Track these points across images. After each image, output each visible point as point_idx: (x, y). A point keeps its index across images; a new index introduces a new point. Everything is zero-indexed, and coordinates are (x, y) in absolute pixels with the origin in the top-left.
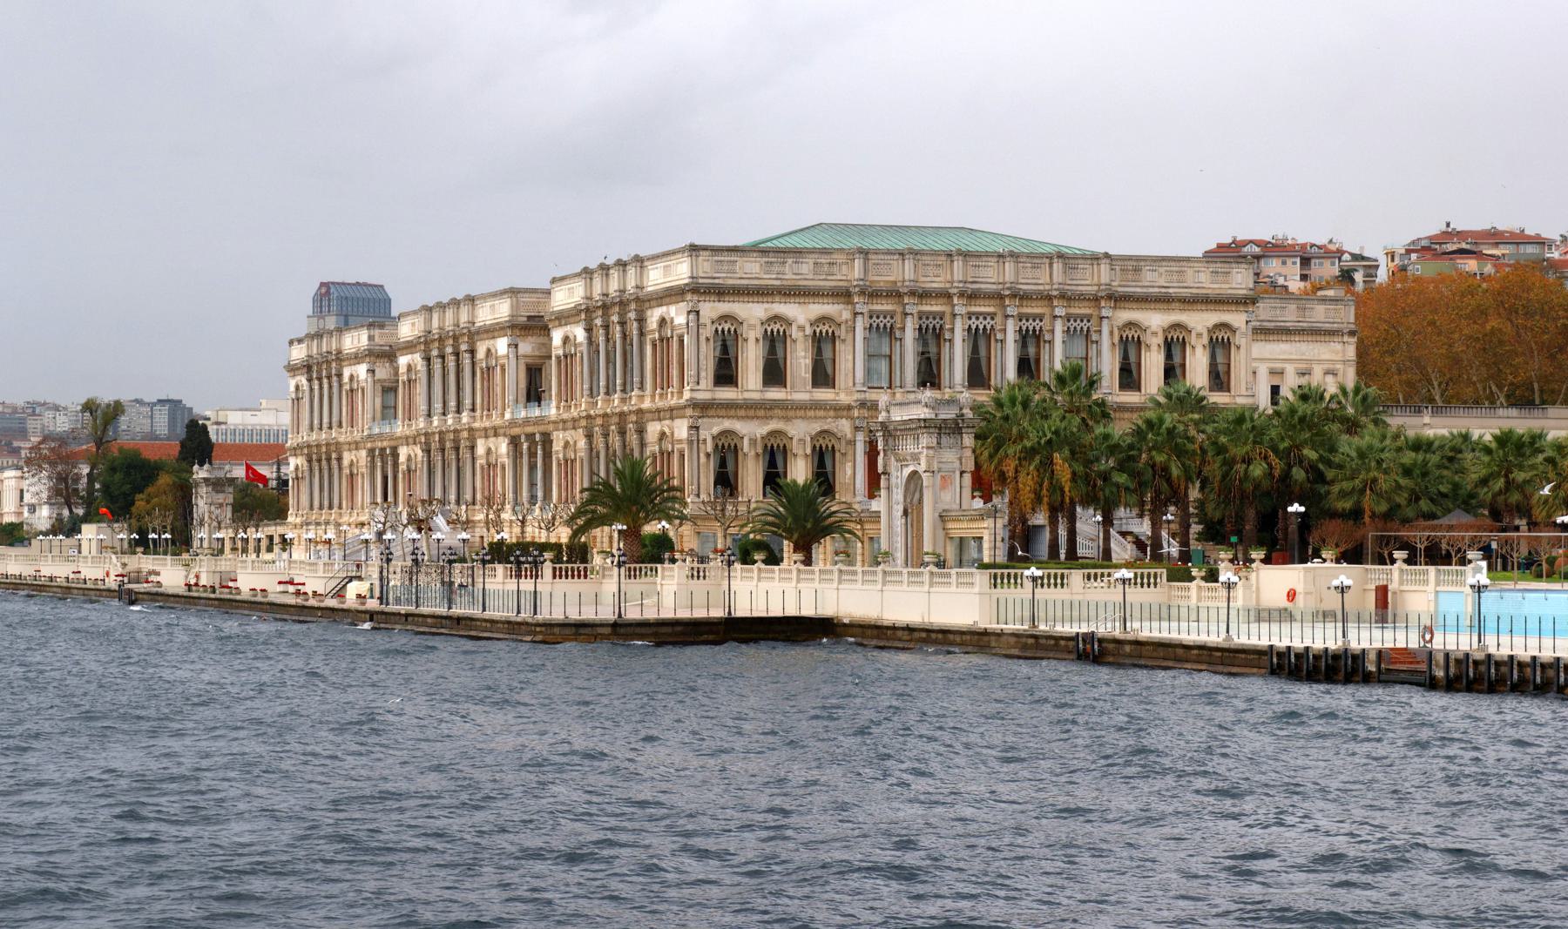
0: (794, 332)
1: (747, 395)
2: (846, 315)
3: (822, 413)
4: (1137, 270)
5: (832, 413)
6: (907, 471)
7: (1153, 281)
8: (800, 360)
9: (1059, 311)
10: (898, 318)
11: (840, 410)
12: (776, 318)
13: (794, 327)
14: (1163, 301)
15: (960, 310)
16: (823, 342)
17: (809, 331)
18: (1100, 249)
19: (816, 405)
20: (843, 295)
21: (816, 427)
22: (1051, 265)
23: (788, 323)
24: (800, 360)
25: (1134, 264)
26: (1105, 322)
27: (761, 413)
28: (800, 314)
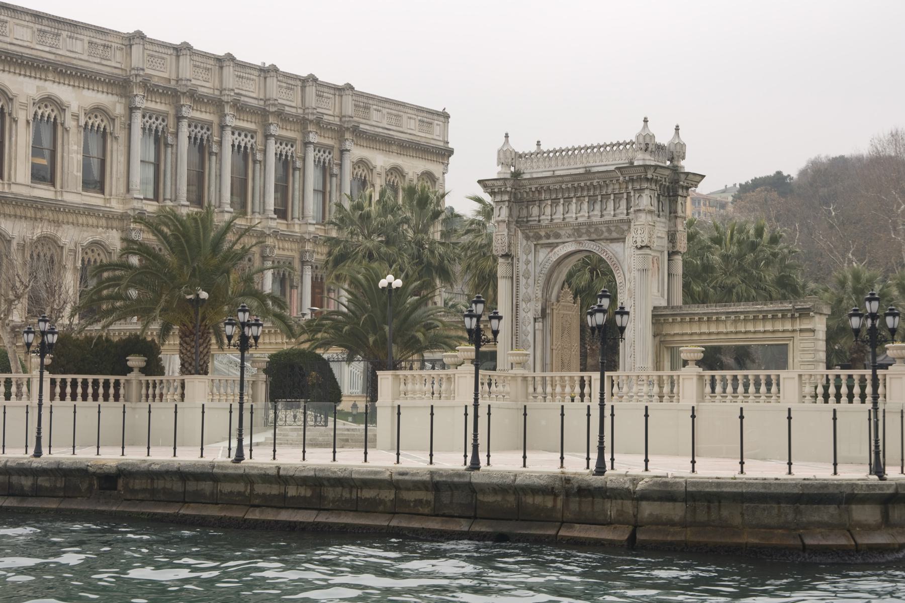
0: (70, 123)
1: (15, 189)
2: (119, 109)
3: (92, 221)
4: (367, 108)
5: (103, 222)
6: (547, 257)
7: (377, 121)
8: (72, 156)
9: (313, 138)
10: (171, 121)
11: (110, 217)
12: (49, 100)
13: (68, 115)
14: (385, 142)
15: (230, 121)
16: (99, 133)
17: (82, 123)
18: (340, 83)
19: (89, 211)
20: (121, 85)
21: (87, 237)
22: (303, 88)
23: (61, 107)
24: (72, 156)
25: (366, 102)
26: (347, 155)
27: (30, 213)
28: (76, 98)
